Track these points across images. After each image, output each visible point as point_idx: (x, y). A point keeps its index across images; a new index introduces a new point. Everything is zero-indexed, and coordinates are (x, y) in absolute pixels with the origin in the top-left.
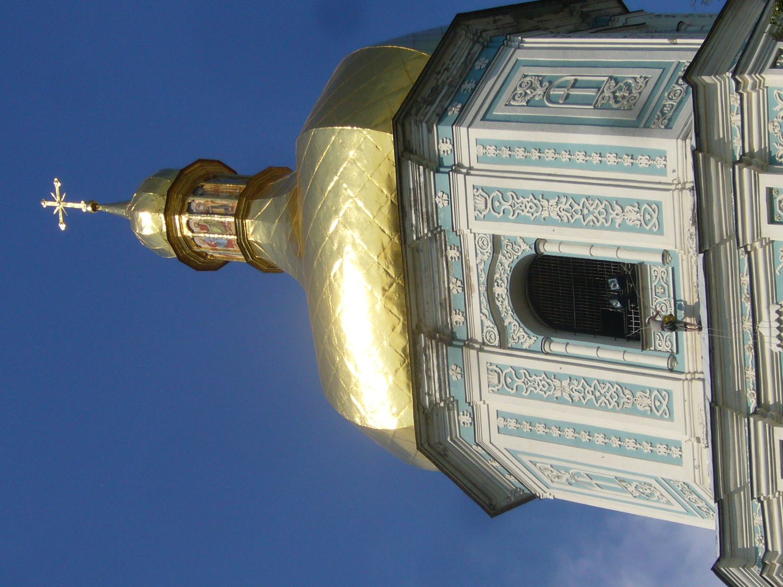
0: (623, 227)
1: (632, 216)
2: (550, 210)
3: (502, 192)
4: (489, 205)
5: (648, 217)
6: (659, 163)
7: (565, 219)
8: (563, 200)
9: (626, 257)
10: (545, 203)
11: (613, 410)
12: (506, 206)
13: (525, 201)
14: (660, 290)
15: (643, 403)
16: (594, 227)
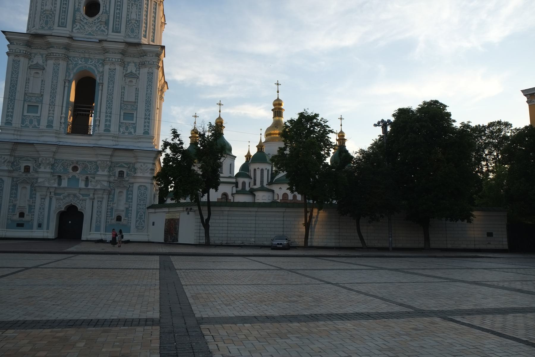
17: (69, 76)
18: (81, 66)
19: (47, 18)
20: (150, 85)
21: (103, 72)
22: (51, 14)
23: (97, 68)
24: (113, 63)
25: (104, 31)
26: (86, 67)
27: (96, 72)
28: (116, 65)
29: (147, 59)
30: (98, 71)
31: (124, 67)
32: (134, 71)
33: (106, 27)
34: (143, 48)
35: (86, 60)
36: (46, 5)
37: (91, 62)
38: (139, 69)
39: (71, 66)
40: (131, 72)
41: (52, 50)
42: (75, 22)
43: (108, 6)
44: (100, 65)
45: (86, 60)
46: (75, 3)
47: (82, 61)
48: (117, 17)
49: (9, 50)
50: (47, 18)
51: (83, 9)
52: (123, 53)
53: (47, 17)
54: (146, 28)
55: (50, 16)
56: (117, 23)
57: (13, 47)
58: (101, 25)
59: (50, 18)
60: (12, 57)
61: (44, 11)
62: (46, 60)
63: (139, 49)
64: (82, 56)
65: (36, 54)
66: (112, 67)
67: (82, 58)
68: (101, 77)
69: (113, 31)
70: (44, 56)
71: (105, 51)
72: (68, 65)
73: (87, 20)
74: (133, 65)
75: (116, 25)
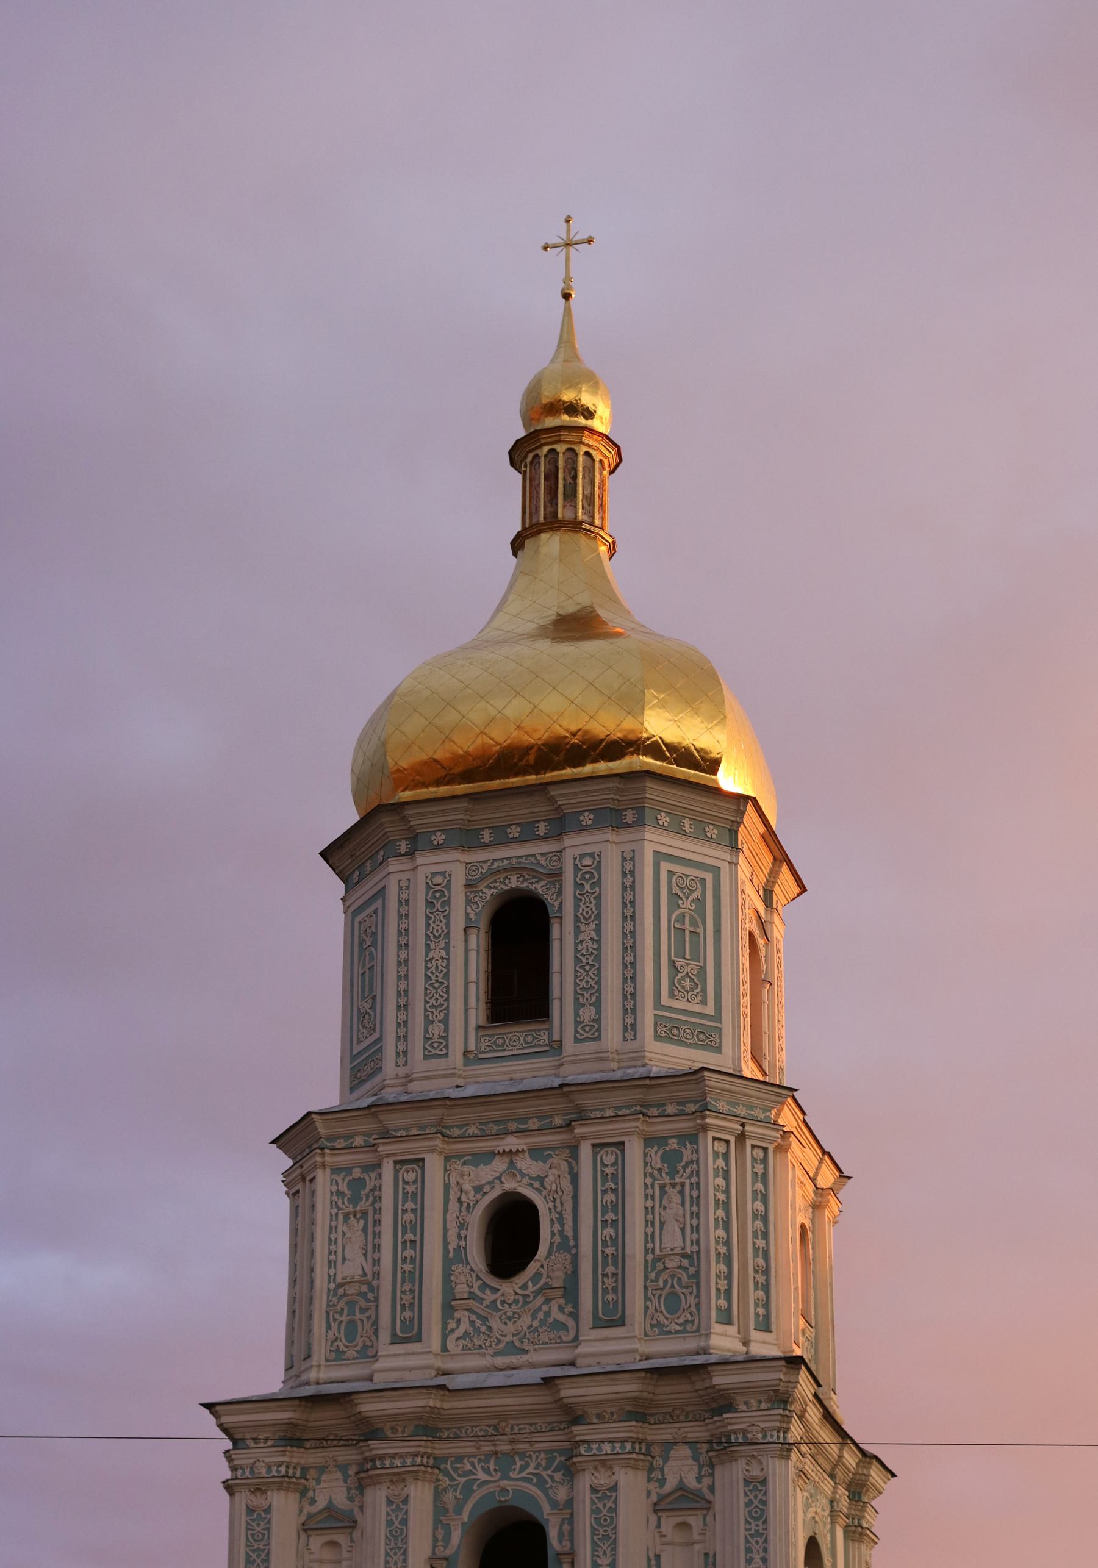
0: (578, 1005)
1: (588, 1014)
2: (588, 932)
3: (598, 883)
4: (588, 869)
5: (587, 1029)
6: (629, 1035)
7: (580, 948)
8: (595, 946)
9: (555, 1007)
10: (593, 926)
11: (426, 1002)
12: (587, 887)
13: (592, 905)
14: (529, 1039)
15: (436, 1030)
16: (576, 977)
17: (447, 1539)
18: (484, 1490)
19: (352, 1312)
20: (758, 1533)
21: (570, 1503)
22: (363, 1295)
23: (545, 1492)
24: (603, 1463)
25: (564, 1327)
26: (503, 1490)
27: (546, 1508)
28: (616, 1469)
29: (736, 1421)
30: (554, 1504)
31: (651, 1469)
32: (691, 1482)
33: (569, 1309)
34: (717, 1381)
35: (505, 1461)
36: (344, 1259)
37: (523, 1469)
38: (712, 1466)
39: (449, 1497)
40: (681, 1488)
41: (379, 1447)
42: (453, 1309)
43: (568, 1217)
44: (558, 1476)
45: (505, 1461)
46: (445, 1230)
47: (487, 1471)
48: (605, 1257)
49: (233, 1469)
50: (352, 1312)
51: (476, 1256)
52: (639, 1412)
53: (351, 1304)
54: (729, 1277)
55: (363, 1303)
56: (610, 1282)
57: (243, 1458)
58: (548, 1301)
59: (363, 1310)
60: (244, 1498)
61: (340, 1285)
62: (361, 1488)
63: (699, 1385)
64: (487, 1448)
65: (322, 1469)
66: (603, 1479)
67: (487, 1457)
68: (566, 1528)
69: (599, 1323)
70: (352, 1471)
71: (574, 1416)
72: (438, 1494)
73: (495, 1290)
74: (686, 1451)
75: (606, 1291)
